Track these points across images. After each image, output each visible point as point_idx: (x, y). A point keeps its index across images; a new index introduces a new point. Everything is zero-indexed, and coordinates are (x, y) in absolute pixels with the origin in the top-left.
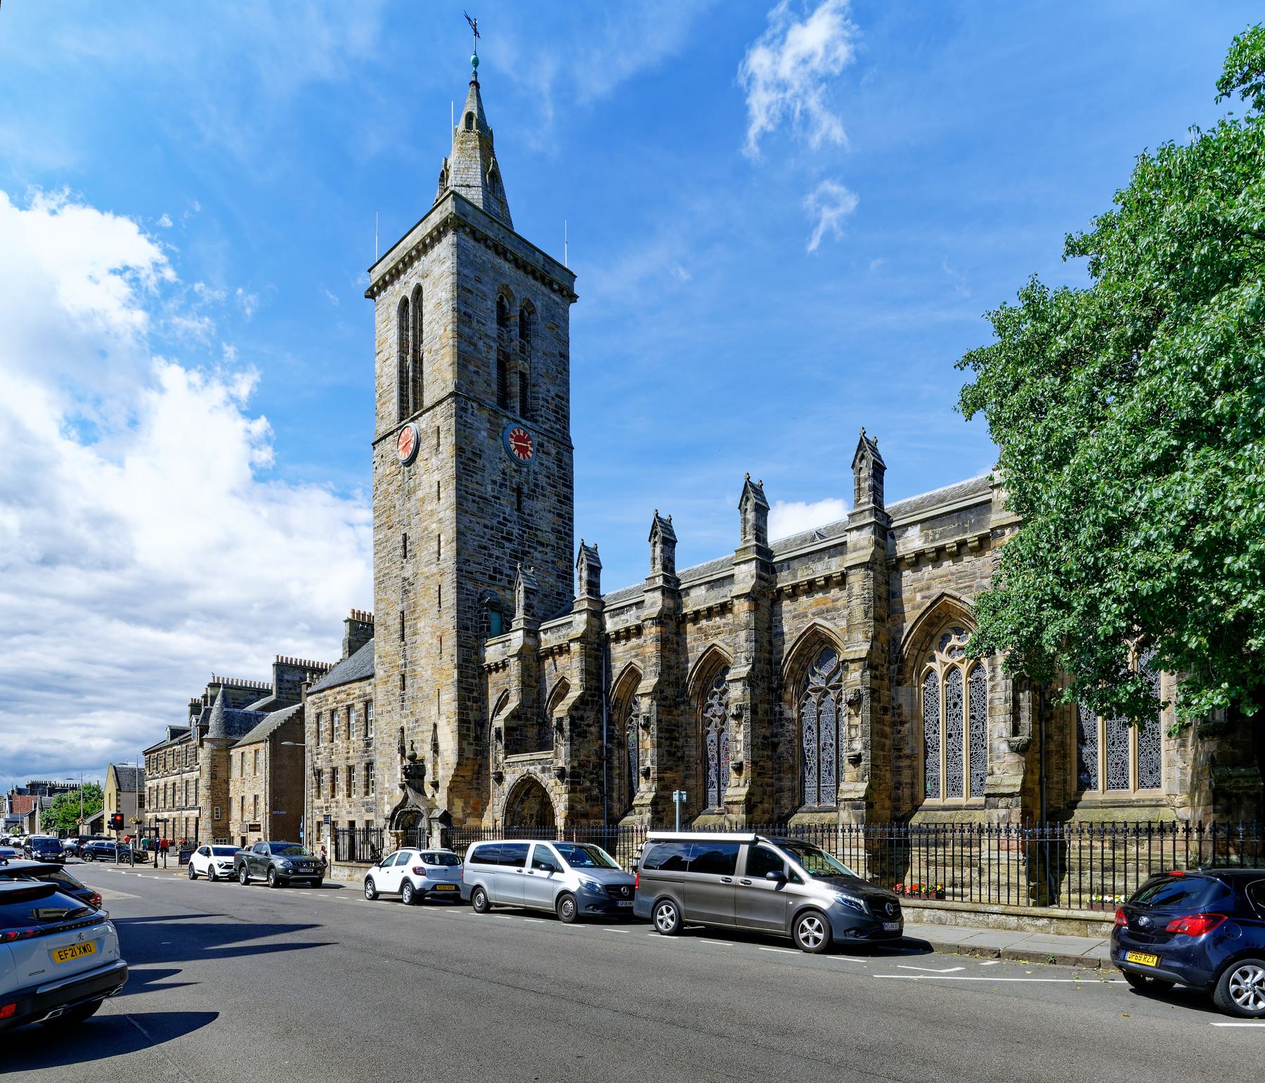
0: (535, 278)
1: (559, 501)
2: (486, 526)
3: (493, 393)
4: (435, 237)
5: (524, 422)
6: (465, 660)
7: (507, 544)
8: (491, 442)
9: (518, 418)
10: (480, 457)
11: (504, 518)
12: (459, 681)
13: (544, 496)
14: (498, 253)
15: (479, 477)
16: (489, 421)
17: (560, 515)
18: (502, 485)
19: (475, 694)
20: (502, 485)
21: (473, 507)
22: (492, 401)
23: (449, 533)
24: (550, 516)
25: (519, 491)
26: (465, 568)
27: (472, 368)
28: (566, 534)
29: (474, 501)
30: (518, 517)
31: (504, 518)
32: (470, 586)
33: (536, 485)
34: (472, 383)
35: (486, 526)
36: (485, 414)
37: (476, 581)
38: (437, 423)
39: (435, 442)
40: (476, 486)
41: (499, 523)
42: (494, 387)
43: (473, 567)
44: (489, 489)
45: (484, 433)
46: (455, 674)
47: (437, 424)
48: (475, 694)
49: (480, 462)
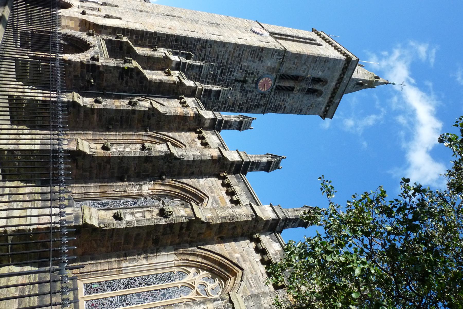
0: (330, 98)
1: (240, 104)
2: (228, 59)
3: (286, 71)
4: (344, 54)
5: (274, 87)
6: (159, 37)
7: (219, 71)
8: (266, 68)
9: (276, 84)
10: (259, 60)
11: (231, 71)
12: (147, 32)
13: (243, 95)
14: (338, 80)
15: (250, 59)
16: (275, 67)
17: (233, 104)
18: (246, 71)
19: (140, 42)
20: (246, 71)
21: (236, 54)
22: (283, 70)
23: (223, 39)
24: (233, 99)
25: (244, 82)
26: (208, 44)
27: (296, 61)
28: (225, 107)
29: (239, 54)
30: (232, 80)
31: (231, 71)
32: (199, 46)
33: (247, 92)
34: (290, 60)
35: (228, 59)
36: (277, 65)
37: (201, 50)
38: (271, 43)
39: (263, 41)
40: (246, 56)
41: (229, 68)
42: (289, 72)
43: (208, 50)
44: (245, 64)
45: (269, 64)
46: (151, 30)
47: (272, 43)
48: (140, 42)
49: (256, 60)
